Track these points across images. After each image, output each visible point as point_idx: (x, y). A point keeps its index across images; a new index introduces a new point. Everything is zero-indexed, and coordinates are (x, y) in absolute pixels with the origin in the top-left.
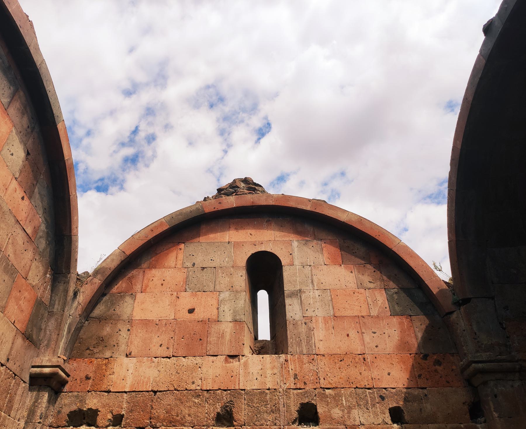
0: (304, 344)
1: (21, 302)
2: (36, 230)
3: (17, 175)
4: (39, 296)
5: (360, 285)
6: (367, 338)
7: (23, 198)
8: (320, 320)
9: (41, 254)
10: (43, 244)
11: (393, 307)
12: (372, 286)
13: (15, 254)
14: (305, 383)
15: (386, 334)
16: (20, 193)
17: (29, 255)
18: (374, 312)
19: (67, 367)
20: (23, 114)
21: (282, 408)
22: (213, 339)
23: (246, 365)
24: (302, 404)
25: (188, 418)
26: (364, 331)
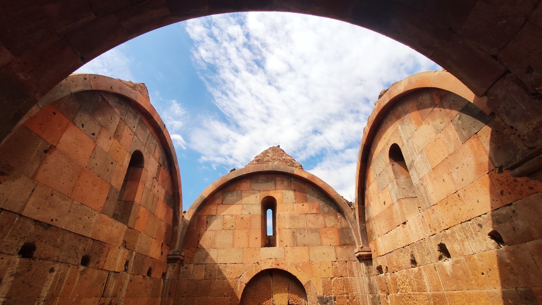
0: (426, 200)
1: (330, 236)
2: (318, 209)
3: (295, 201)
4: (339, 227)
5: (438, 131)
6: (454, 175)
7: (303, 205)
8: (427, 177)
9: (329, 213)
10: (326, 209)
11: (461, 134)
12: (442, 126)
13: (313, 224)
14: (435, 230)
15: (465, 165)
16: (300, 205)
17: (321, 218)
18: (452, 150)
19: (365, 248)
20: (283, 183)
21: (431, 251)
22: (395, 216)
23: (410, 227)
24: (439, 245)
25: (403, 265)
26: (451, 170)
